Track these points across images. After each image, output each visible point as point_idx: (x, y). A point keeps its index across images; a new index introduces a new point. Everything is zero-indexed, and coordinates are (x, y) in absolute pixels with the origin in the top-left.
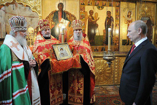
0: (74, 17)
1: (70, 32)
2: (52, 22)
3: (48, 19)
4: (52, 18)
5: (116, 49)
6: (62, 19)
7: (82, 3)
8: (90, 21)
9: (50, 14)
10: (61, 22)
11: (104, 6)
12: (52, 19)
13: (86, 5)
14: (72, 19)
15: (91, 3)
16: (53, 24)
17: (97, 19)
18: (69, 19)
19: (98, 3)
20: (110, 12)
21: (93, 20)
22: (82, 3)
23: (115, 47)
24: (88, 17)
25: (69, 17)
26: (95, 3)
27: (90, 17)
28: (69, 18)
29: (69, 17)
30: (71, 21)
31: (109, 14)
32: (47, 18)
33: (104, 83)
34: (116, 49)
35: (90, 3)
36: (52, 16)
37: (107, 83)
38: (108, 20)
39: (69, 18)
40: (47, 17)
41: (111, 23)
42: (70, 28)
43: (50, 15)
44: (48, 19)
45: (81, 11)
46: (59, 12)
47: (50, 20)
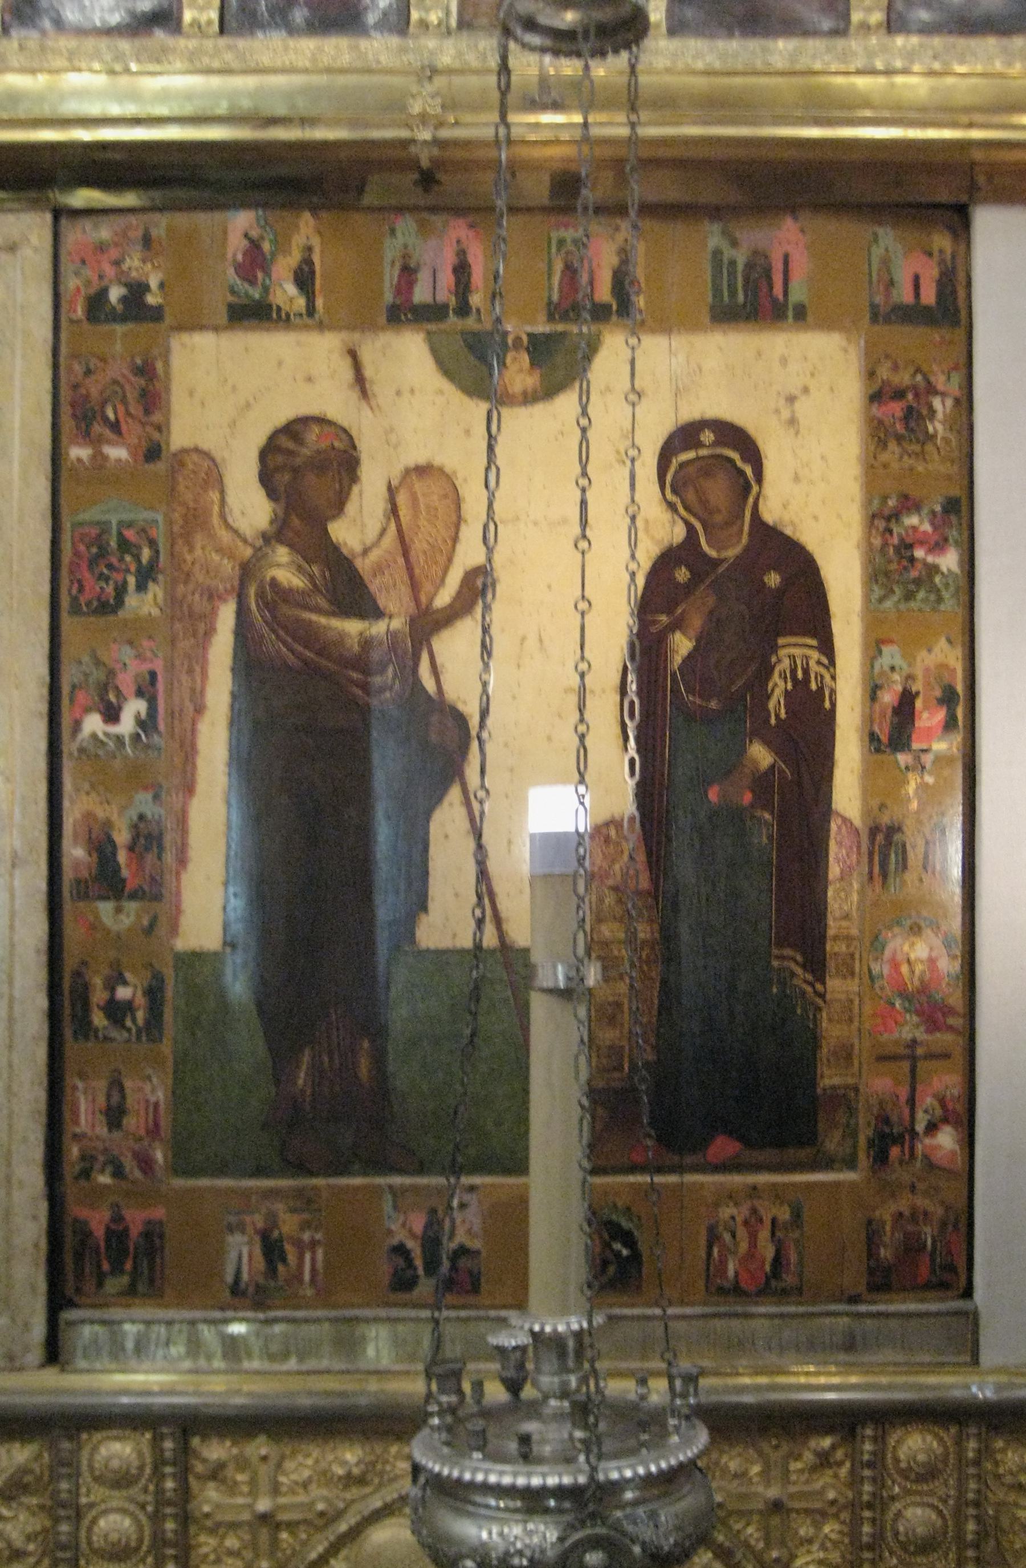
7: (115, 294)
8: (274, 645)
11: (601, 313)
13: (193, 324)
15: (304, 279)
17: (444, 598)
19: (462, 269)
21: (352, 627)
22: (115, 294)
23: (890, 1190)
24: (228, 568)
26: (391, 275)
27: (282, 554)
34: (912, 1247)
35: (284, 267)
38: (697, 622)
45: (79, 453)
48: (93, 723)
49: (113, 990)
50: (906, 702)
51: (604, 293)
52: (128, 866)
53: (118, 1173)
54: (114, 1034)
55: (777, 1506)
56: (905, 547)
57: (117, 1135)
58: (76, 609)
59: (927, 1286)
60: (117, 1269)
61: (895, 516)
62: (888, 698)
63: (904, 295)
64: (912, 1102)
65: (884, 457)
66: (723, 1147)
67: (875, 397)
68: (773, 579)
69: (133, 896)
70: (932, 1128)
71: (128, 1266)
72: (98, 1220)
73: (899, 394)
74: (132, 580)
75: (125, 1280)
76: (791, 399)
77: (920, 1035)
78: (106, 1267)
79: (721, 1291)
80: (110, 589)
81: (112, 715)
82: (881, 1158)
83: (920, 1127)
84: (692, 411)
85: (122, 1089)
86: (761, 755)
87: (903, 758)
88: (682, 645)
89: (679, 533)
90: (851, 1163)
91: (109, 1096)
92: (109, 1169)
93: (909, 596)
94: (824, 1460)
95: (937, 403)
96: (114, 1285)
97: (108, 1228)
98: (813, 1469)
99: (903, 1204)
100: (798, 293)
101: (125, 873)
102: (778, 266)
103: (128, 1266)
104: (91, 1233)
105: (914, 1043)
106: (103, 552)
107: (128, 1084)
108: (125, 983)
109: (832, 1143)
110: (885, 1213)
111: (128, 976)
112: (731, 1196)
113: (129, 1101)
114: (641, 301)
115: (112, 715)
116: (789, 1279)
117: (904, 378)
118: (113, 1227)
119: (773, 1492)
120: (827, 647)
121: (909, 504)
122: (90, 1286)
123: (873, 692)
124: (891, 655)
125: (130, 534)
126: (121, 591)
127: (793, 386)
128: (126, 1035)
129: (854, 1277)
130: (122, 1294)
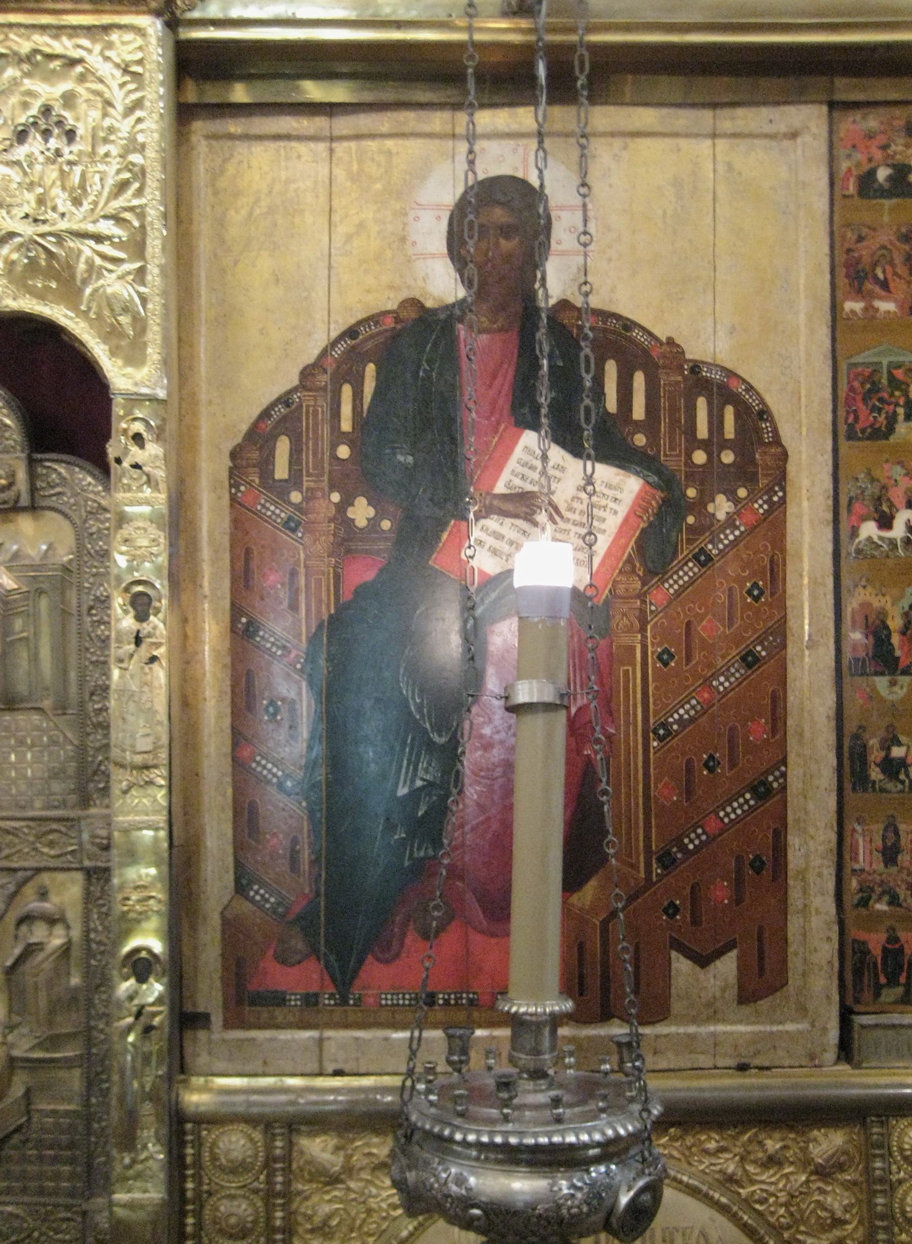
0: (730, 397)
1: (665, 658)
2: (347, 502)
3: (283, 446)
4: (346, 426)
6: (529, 438)
7: (882, 174)
9: (307, 373)
10: (500, 488)
12: (344, 452)
14: (705, 445)
16: (373, 523)
18: (640, 440)
22: (882, 174)
25: (639, 412)
28: (651, 424)
29: (639, 412)
30: (672, 462)
32: (272, 438)
36: (358, 395)
39: (638, 426)
40: (266, 414)
42: (671, 587)
43: (323, 379)
44: (283, 446)
45: (853, 306)
46: (462, 330)
47: (308, 459)
48: (869, 529)
49: (889, 749)
52: (901, 648)
53: (894, 901)
54: (890, 786)
57: (893, 870)
58: (851, 436)
60: (893, 981)
69: (905, 672)
71: (903, 979)
72: (876, 941)
74: (901, 411)
75: (900, 990)
78: (883, 980)
80: (882, 418)
81: (886, 522)
85: (897, 833)
91: (884, 838)
92: (886, 898)
96: (890, 995)
97: (884, 949)
101: (898, 653)
103: (903, 979)
104: (869, 952)
106: (875, 388)
107: (902, 827)
108: (900, 744)
111: (903, 739)
113: (903, 842)
115: (886, 522)
118: (890, 947)
122: (867, 995)
125: (899, 374)
126: (892, 420)
128: (900, 786)
130: (896, 1002)
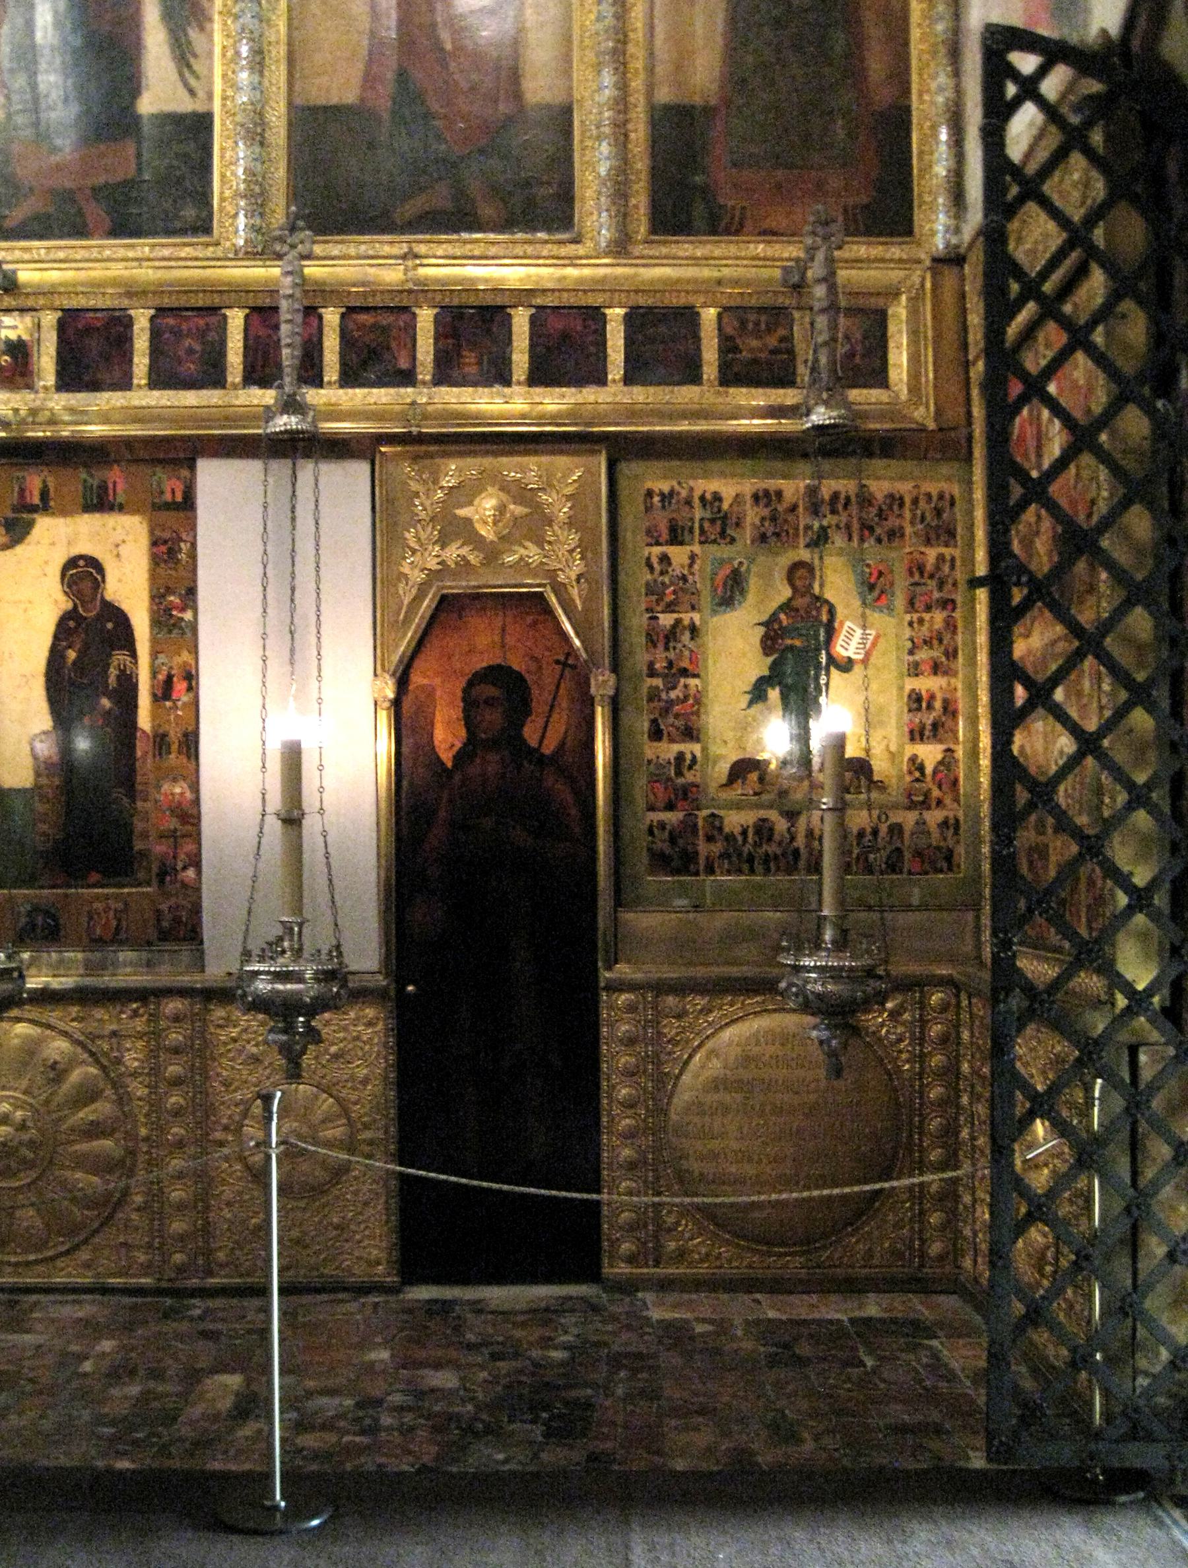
5: (177, 920)
11: (33, 509)
20: (94, 563)
23: (167, 895)
31: (86, 585)
33: (60, 1263)
34: (177, 920)
37: (87, 1265)
41: (108, 665)
50: (169, 680)
51: (36, 500)
55: (114, 1034)
56: (168, 611)
59: (184, 939)
61: (163, 596)
62: (161, 677)
63: (168, 497)
64: (175, 857)
65: (159, 570)
66: (95, 877)
67: (154, 543)
68: (110, 626)
70: (185, 868)
73: (165, 542)
76: (117, 546)
77: (178, 826)
79: (93, 941)
82: (162, 882)
83: (180, 865)
84: (76, 551)
86: (106, 703)
87: (168, 704)
88: (72, 655)
89: (70, 606)
90: (149, 884)
93: (170, 632)
94: (135, 1014)
95: (182, 545)
98: (131, 1018)
99: (173, 901)
100: (121, 498)
102: (111, 486)
105: (175, 830)
109: (141, 875)
110: (164, 907)
112: (97, 898)
114: (52, 503)
116: (123, 936)
117: (167, 535)
119: (114, 1027)
120: (134, 655)
121: (169, 590)
123: (154, 673)
124: (162, 658)
127: (118, 539)
129: (152, 933)
